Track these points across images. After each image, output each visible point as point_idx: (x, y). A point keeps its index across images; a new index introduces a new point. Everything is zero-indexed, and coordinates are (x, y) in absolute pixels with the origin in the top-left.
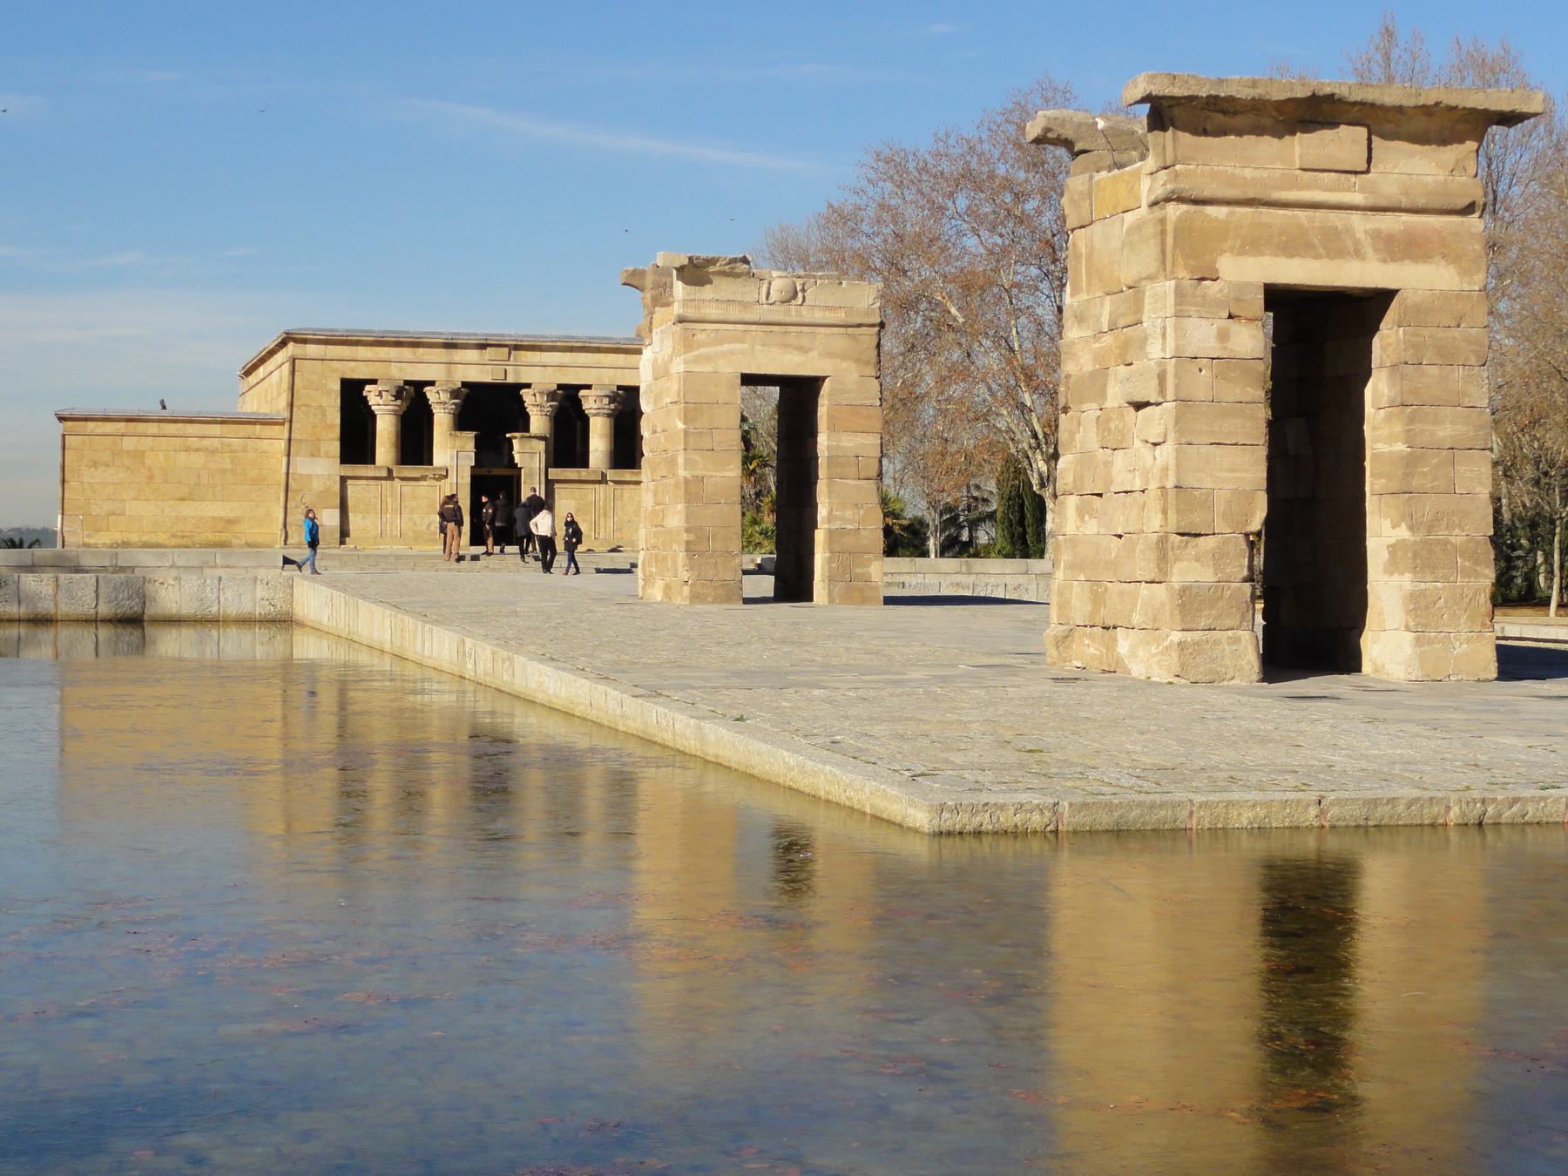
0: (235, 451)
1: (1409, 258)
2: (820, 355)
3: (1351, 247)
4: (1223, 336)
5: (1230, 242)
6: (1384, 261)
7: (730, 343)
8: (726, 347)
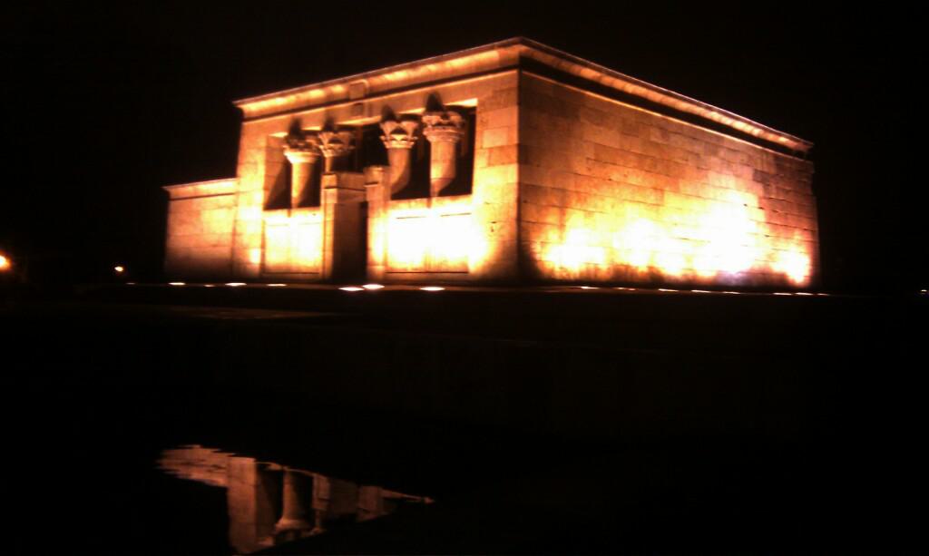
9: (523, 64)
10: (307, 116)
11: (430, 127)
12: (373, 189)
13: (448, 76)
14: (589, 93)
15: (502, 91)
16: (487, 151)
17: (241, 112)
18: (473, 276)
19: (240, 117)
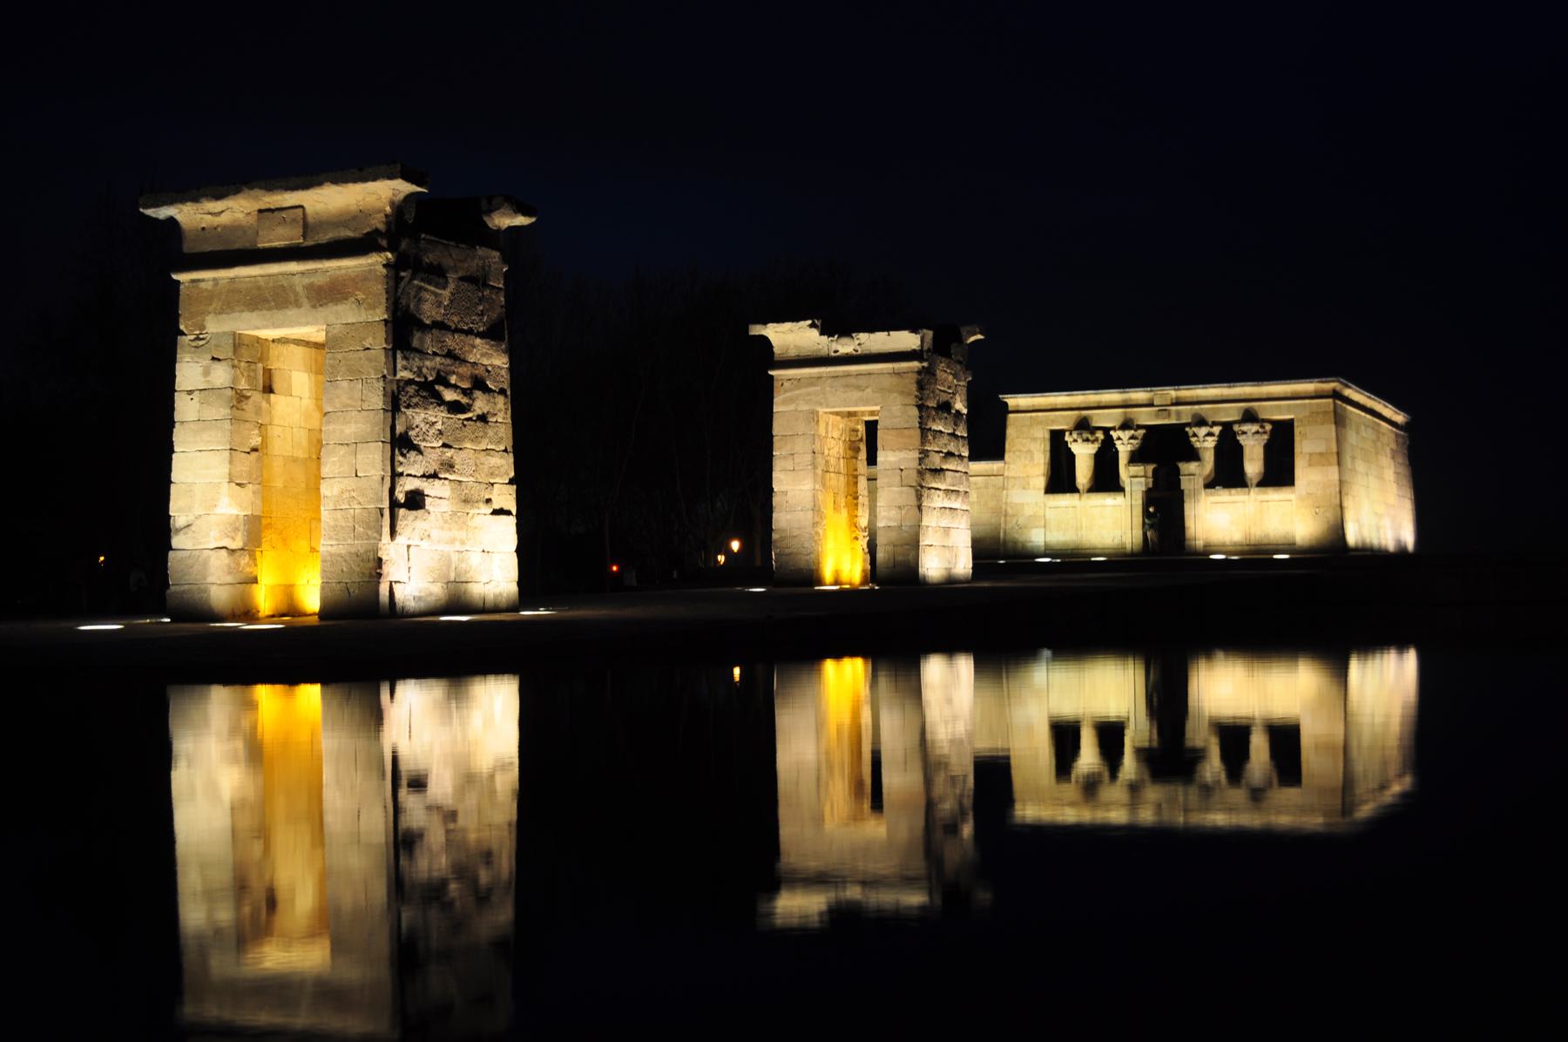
0: (980, 488)
1: (332, 301)
2: (873, 392)
3: (292, 299)
4: (206, 373)
5: (214, 305)
6: (314, 307)
7: (806, 387)
8: (803, 391)
9: (1336, 395)
10: (1098, 414)
11: (1249, 434)
12: (1190, 480)
13: (1264, 397)
14: (1349, 408)
15: (1318, 413)
16: (1307, 457)
17: (1006, 404)
18: (1301, 547)
19: (1004, 410)
